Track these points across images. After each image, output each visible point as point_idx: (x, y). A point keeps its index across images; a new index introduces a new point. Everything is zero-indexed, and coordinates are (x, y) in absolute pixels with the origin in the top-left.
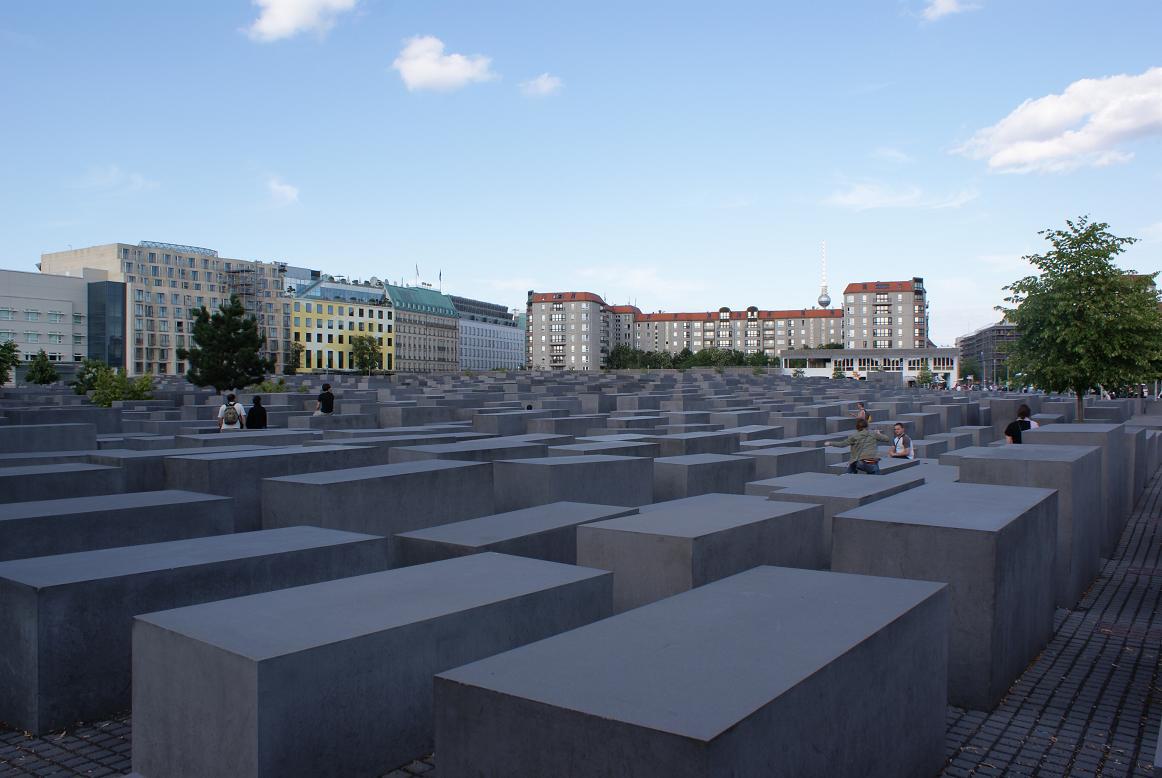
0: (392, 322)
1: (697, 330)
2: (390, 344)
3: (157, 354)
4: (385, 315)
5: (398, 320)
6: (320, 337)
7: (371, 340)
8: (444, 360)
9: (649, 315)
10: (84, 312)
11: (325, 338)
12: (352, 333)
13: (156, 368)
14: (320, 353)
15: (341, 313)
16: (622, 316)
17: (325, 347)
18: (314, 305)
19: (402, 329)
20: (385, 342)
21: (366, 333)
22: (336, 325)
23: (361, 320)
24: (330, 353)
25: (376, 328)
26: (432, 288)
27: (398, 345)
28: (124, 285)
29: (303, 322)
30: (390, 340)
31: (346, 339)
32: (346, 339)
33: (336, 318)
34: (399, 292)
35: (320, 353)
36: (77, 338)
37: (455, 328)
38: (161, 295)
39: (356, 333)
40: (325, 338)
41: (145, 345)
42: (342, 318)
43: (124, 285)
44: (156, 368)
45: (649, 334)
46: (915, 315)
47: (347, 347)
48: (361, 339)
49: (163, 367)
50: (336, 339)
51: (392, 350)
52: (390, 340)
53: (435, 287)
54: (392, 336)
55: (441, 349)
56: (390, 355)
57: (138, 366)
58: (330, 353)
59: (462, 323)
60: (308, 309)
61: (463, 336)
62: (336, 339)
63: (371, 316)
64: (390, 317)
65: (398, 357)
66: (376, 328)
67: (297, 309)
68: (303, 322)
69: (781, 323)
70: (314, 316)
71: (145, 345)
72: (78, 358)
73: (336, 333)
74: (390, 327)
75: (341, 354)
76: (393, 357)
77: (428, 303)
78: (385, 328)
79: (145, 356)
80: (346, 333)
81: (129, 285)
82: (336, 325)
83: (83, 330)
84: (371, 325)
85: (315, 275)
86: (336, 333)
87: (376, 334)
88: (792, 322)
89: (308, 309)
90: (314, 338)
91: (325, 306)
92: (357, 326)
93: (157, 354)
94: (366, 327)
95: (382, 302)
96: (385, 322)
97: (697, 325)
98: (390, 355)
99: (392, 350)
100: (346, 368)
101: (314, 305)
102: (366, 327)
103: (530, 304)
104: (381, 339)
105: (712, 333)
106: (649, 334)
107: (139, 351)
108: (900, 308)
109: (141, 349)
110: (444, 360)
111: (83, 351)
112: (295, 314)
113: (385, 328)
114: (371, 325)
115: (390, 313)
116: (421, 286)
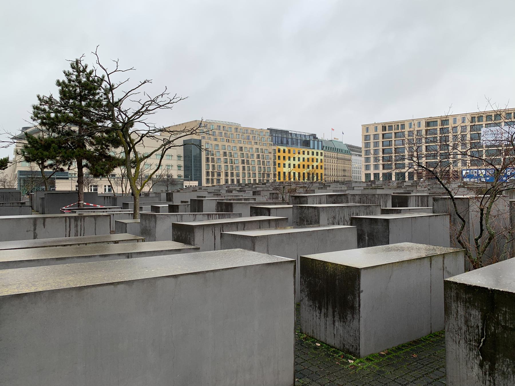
0: (322, 157)
2: (321, 168)
3: (216, 174)
5: (325, 156)
8: (345, 176)
10: (182, 155)
13: (215, 181)
14: (290, 173)
20: (319, 167)
23: (308, 156)
24: (294, 173)
25: (315, 160)
26: (339, 140)
27: (325, 169)
28: (200, 140)
29: (282, 158)
30: (321, 166)
36: (179, 166)
37: (350, 160)
38: (217, 145)
41: (211, 170)
43: (200, 140)
44: (215, 181)
49: (218, 181)
52: (321, 166)
53: (340, 140)
54: (322, 164)
55: (344, 170)
56: (321, 174)
57: (208, 180)
58: (294, 173)
64: (321, 155)
65: (325, 175)
66: (315, 160)
67: (279, 151)
68: (282, 158)
71: (211, 170)
72: (179, 176)
74: (321, 160)
75: (299, 173)
76: (323, 175)
77: (339, 148)
78: (319, 161)
79: (393, 157)
81: (203, 143)
83: (182, 163)
84: (313, 159)
87: (315, 164)
93: (216, 174)
94: (311, 160)
96: (319, 157)
98: (321, 174)
99: (323, 171)
100: (301, 180)
102: (311, 160)
107: (208, 173)
110: (345, 176)
111: (182, 173)
112: (277, 154)
113: (319, 161)
114: (313, 159)
115: (321, 153)
116: (333, 139)
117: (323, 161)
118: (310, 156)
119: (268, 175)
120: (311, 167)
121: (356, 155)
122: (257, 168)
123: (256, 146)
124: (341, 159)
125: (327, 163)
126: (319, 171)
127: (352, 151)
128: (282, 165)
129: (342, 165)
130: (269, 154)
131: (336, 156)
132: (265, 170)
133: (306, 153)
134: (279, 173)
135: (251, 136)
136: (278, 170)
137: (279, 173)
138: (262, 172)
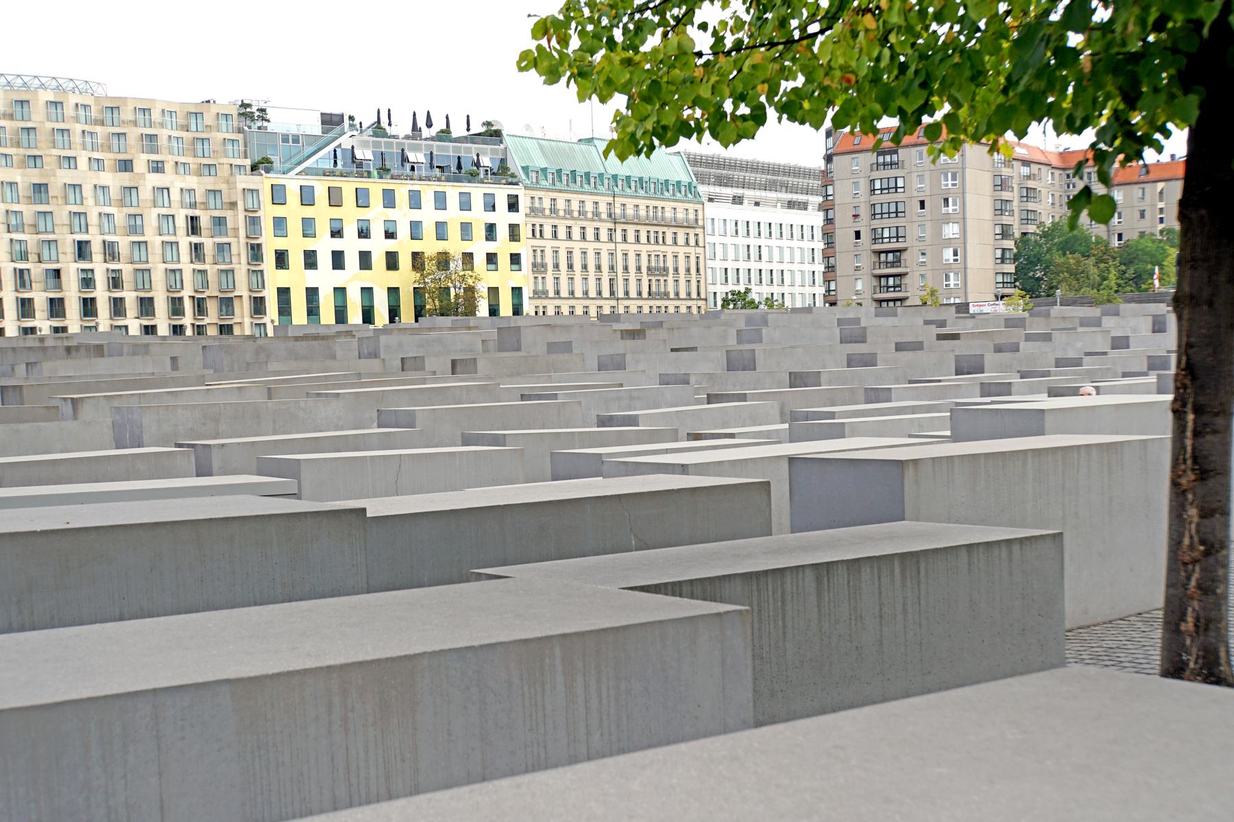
4: (502, 203)
5: (534, 211)
6: (338, 260)
7: (468, 257)
11: (352, 260)
12: (417, 246)
15: (465, 205)
17: (353, 279)
18: (321, 188)
19: (548, 232)
21: (455, 246)
22: (377, 231)
23: (441, 216)
24: (367, 292)
27: (539, 267)
30: (515, 259)
31: (405, 261)
32: (405, 261)
33: (377, 215)
34: (541, 147)
39: (430, 246)
40: (352, 260)
42: (391, 214)
47: (405, 278)
48: (443, 261)
50: (378, 260)
52: (515, 259)
56: (517, 291)
58: (367, 292)
59: (711, 210)
60: (307, 197)
61: (716, 239)
62: (378, 260)
63: (465, 205)
64: (513, 206)
65: (539, 294)
66: (479, 232)
67: (278, 196)
70: (322, 213)
73: (378, 246)
75: (393, 292)
80: (404, 247)
82: (377, 231)
85: (331, 121)
86: (378, 246)
87: (480, 248)
89: (307, 197)
90: (325, 260)
91: (348, 187)
92: (429, 230)
94: (454, 231)
95: (502, 172)
96: (503, 219)
98: (517, 291)
99: (523, 278)
101: (321, 188)
102: (454, 231)
103: (829, 159)
104: (491, 258)
109: (181, 299)
110: (665, 296)
112: (268, 212)
113: (502, 232)
117: (525, 232)
118: (453, 215)
119: (227, 304)
120: (456, 265)
121: (738, 200)
122: (158, 277)
123: (155, 180)
125: (549, 245)
126: (504, 278)
127: (722, 182)
128: (296, 259)
129: (644, 249)
130: (228, 214)
131: (603, 208)
132: (206, 285)
133: (428, 198)
134: (284, 293)
135: (133, 133)
136: (275, 278)
137: (284, 293)
138: (186, 293)
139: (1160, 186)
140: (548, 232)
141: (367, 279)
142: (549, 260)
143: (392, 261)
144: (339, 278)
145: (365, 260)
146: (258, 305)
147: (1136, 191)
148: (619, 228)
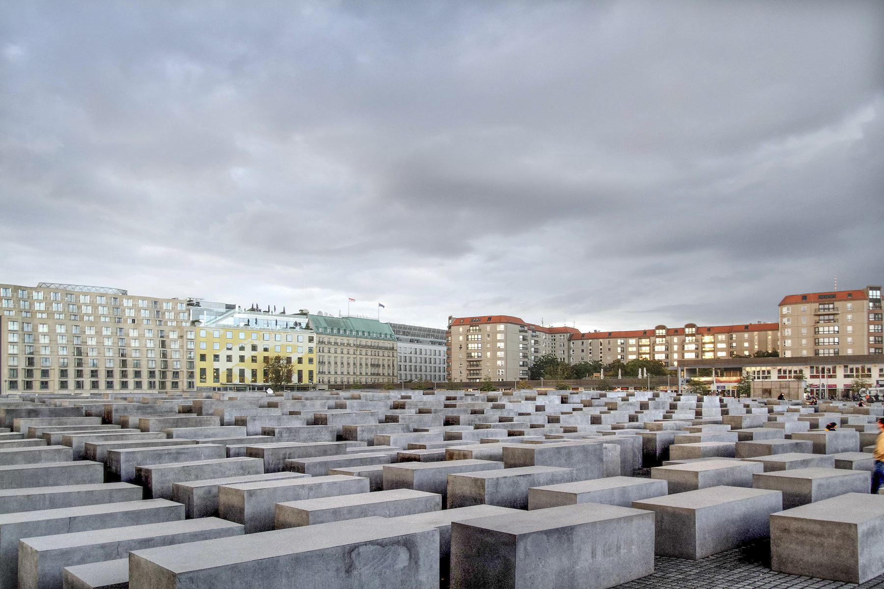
1: (632, 346)
9: (583, 335)
14: (230, 371)
16: (558, 336)
19: (326, 350)
27: (321, 363)
35: (230, 371)
45: (583, 351)
46: (870, 323)
47: (260, 367)
51: (314, 367)
59: (400, 344)
69: (722, 337)
88: (734, 336)
97: (632, 341)
98: (311, 372)
99: (314, 367)
105: (648, 348)
106: (583, 351)
108: (849, 317)
124: (370, 347)
134: (203, 371)
139: (590, 341)
140: (326, 350)
141: (242, 366)
142: (326, 360)
143: (254, 359)
144: (229, 365)
145: (242, 359)
146: (191, 375)
147: (580, 342)
148: (359, 349)
